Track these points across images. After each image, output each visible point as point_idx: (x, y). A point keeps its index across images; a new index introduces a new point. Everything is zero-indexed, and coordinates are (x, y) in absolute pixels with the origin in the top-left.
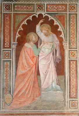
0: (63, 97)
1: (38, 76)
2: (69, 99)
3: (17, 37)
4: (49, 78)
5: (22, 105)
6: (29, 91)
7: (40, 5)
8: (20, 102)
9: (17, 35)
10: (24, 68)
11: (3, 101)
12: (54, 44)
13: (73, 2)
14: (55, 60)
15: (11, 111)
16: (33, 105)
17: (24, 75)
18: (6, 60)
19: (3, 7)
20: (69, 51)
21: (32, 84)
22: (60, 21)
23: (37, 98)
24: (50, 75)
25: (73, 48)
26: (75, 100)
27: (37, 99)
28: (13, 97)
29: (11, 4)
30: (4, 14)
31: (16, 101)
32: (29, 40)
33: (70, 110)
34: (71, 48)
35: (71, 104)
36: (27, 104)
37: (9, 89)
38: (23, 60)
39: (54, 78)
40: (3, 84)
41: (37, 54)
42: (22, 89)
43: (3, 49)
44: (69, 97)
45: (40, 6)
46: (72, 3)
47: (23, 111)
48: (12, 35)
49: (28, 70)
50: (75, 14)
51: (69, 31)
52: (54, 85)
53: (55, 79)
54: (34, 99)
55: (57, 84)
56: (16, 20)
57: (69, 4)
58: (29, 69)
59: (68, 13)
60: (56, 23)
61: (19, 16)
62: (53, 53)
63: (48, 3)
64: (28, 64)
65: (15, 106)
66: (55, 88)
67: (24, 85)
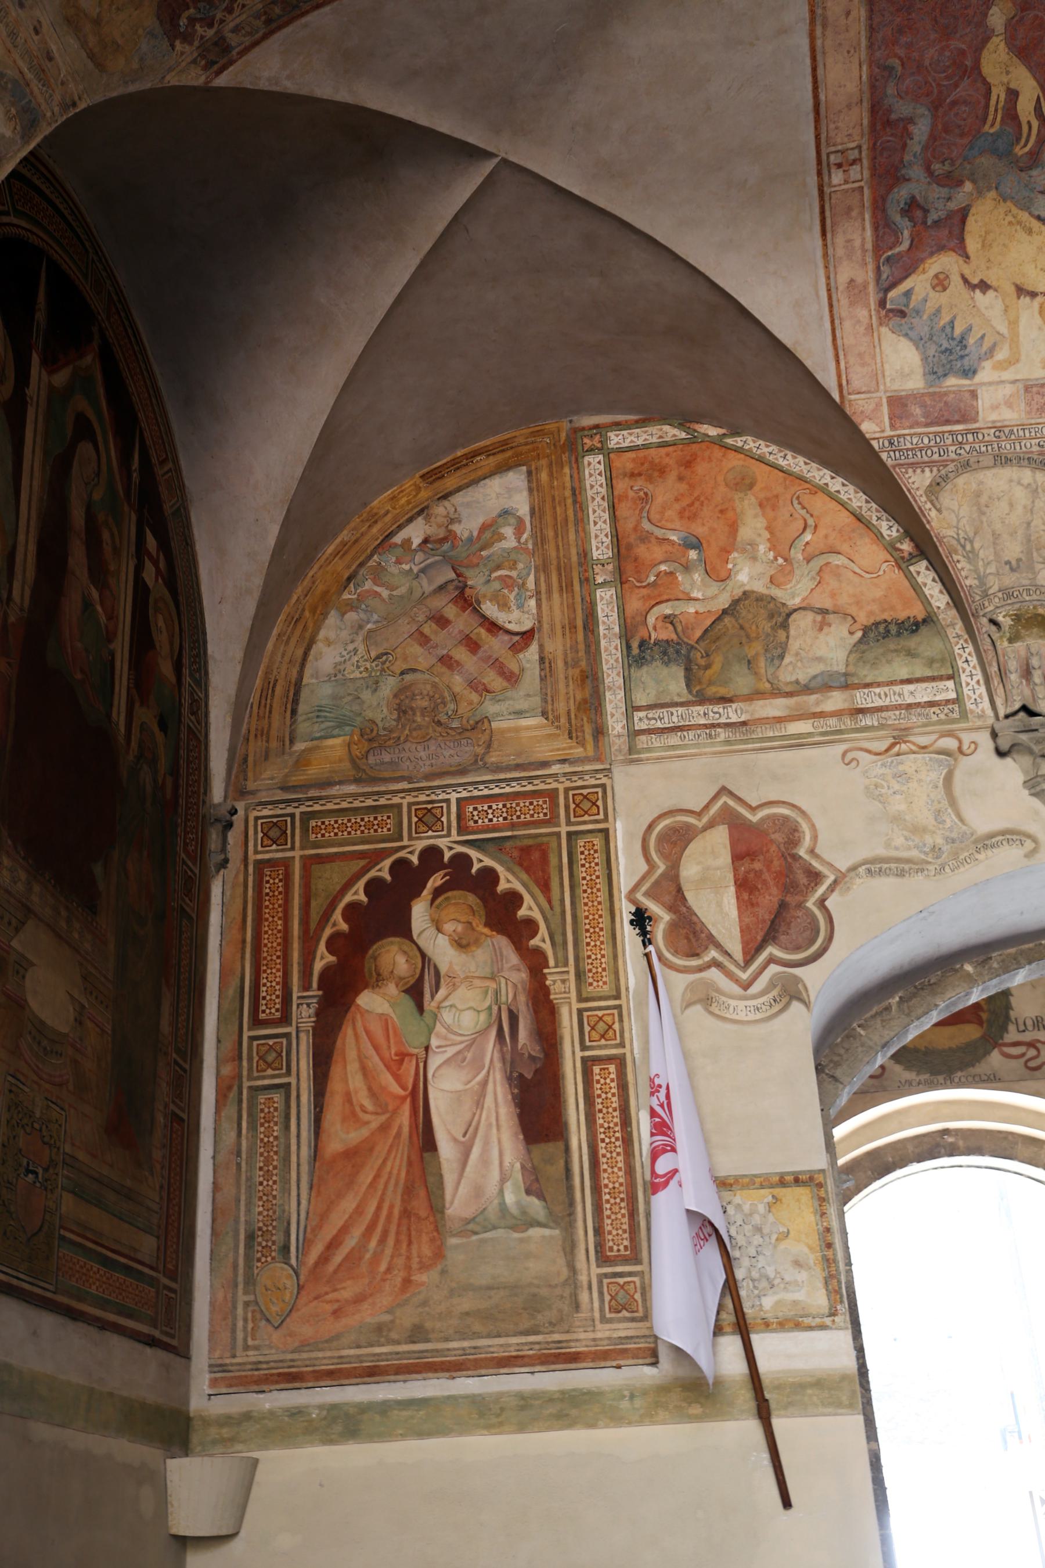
0: (561, 1261)
1: (426, 1155)
2: (595, 1271)
3: (318, 966)
4: (485, 1161)
5: (344, 1321)
6: (383, 1240)
7: (429, 806)
8: (336, 1306)
9: (322, 958)
10: (352, 1117)
11: (247, 1304)
12: (503, 985)
13: (587, 777)
14: (512, 1062)
15: (289, 1356)
16: (407, 1318)
17: (354, 1156)
18: (266, 1082)
19: (256, 833)
20: (580, 1012)
21: (395, 1199)
22: (527, 870)
23: (424, 1278)
24: (486, 1143)
25: (601, 999)
26: (631, 1274)
27: (423, 1284)
28: (302, 1278)
29: (292, 816)
30: (260, 865)
31: (316, 1298)
32: (379, 975)
33: (607, 1334)
35: (607, 1298)
36: (368, 1315)
37: (278, 1237)
38: (349, 1077)
39: (508, 1159)
40: (248, 1211)
41: (423, 1040)
42: (344, 1230)
43: (249, 1029)
44: (597, 1259)
45: (429, 810)
46: (580, 783)
47: (352, 1352)
48: (296, 956)
49: (374, 1125)
50: (600, 831)
51: (574, 916)
52: (510, 1198)
53: (518, 1166)
54: (407, 1282)
55: (528, 1192)
56: (313, 887)
58: (383, 1118)
59: (564, 829)
60: (508, 881)
61: (328, 866)
62: (500, 1029)
63: (464, 794)
64: (373, 1094)
65: (307, 1331)
66: (514, 1211)
67: (354, 1206)
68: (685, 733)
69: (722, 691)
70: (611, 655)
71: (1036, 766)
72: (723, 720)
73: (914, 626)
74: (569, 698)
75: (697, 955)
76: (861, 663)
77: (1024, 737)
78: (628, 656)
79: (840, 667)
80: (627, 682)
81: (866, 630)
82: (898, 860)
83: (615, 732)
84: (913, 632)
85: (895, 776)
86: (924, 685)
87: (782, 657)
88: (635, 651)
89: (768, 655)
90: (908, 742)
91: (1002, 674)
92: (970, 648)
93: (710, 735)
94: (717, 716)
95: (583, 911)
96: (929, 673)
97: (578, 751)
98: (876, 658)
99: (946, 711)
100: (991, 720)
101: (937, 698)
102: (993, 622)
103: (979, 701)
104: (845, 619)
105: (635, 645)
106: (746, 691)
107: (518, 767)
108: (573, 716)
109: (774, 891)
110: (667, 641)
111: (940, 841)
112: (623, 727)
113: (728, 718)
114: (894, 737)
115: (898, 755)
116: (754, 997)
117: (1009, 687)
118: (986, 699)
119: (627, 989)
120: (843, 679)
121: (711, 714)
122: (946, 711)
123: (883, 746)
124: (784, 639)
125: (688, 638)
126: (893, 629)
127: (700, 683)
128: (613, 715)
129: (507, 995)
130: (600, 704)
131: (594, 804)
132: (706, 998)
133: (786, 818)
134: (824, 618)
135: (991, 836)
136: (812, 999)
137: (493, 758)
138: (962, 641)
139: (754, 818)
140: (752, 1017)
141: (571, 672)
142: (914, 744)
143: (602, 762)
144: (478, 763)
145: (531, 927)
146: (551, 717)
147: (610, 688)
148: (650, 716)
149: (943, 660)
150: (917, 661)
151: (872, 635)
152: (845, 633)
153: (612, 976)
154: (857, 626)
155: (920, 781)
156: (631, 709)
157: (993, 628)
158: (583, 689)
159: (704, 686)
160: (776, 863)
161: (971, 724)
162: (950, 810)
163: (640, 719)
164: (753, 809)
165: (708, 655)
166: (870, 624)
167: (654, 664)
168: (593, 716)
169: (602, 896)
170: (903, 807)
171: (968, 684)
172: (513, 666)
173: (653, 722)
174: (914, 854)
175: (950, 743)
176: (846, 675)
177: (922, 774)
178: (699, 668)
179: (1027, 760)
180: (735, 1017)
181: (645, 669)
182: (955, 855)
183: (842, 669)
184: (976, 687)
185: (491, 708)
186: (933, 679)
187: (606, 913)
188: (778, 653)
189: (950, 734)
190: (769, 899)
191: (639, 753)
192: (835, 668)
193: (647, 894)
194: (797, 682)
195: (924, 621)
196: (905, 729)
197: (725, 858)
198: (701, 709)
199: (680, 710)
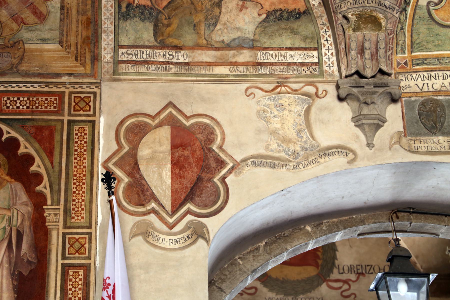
12: (15, 214)
13: (84, 87)
14: (16, 264)
20: (64, 235)
22: (39, 142)
25: (78, 227)
34: (70, 227)
46: (80, 90)
50: (90, 121)
51: (67, 174)
57: (70, 93)
59: (66, 118)
60: (26, 147)
62: (10, 243)
68: (150, 66)
69: (176, 42)
70: (108, 10)
71: (360, 109)
72: (175, 60)
73: (297, 15)
74: (78, 35)
75: (143, 205)
76: (263, 35)
77: (355, 90)
78: (119, 13)
79: (250, 35)
80: (117, 29)
81: (269, 14)
82: (272, 158)
83: (106, 60)
84: (297, 18)
85: (276, 106)
86: (300, 52)
87: (215, 25)
88: (124, 10)
89: (207, 23)
90: (287, 86)
91: (347, 50)
92: (330, 33)
93: (166, 69)
94: (171, 57)
95: (73, 171)
96: (303, 45)
97: (81, 69)
98: (273, 32)
99: (311, 69)
100: (337, 78)
101: (307, 61)
102: (345, 17)
103: (331, 65)
104: (257, 5)
105: (124, 5)
106: (191, 43)
107: (40, 75)
108: (79, 47)
109: (195, 169)
110: (145, 6)
111: (298, 148)
112: (111, 58)
113: (178, 59)
114: (278, 82)
115: (279, 93)
116: (175, 234)
117: (350, 58)
118: (336, 65)
119: (96, 223)
120: (251, 43)
121: (168, 56)
122: (311, 69)
123: (270, 87)
124: (218, 14)
125: (158, 6)
126: (285, 15)
127: (163, 35)
128: (105, 49)
129: (17, 220)
130: (98, 41)
131: (88, 104)
132: (146, 233)
133: (207, 125)
134: (244, 3)
135: (329, 148)
136: (211, 238)
137: (23, 67)
138: (325, 28)
139: (188, 124)
140: (172, 246)
141: (80, 18)
142: (289, 88)
143: (95, 78)
144: (13, 69)
145: (38, 178)
146: (65, 45)
147: (105, 32)
148: (129, 52)
149: (313, 38)
150: (297, 37)
151: (272, 18)
152: (256, 14)
153: (88, 214)
154: (263, 11)
155: (290, 111)
156: (117, 46)
157: (345, 21)
158: (88, 30)
159: (165, 38)
160: (198, 152)
161: (325, 79)
162: (306, 130)
163: (123, 54)
164: (187, 118)
165: (169, 18)
166: (271, 10)
167: (135, 19)
168: (92, 48)
169: (87, 163)
170: (278, 126)
171: (326, 54)
172: (43, 9)
173: (131, 56)
174: (282, 155)
175: (311, 89)
176: (253, 40)
177: (293, 106)
178: (163, 26)
179: (355, 104)
180: (162, 245)
181: (129, 22)
182: (306, 158)
183: (251, 36)
184: (331, 56)
185: (25, 34)
186: (305, 49)
187: (88, 174)
188: (214, 22)
189: (311, 84)
190: (191, 174)
191: (120, 75)
192: (247, 36)
193: (115, 164)
194: (223, 41)
195: (304, 12)
196: (285, 78)
197: (167, 146)
198: (161, 52)
199: (149, 51)
